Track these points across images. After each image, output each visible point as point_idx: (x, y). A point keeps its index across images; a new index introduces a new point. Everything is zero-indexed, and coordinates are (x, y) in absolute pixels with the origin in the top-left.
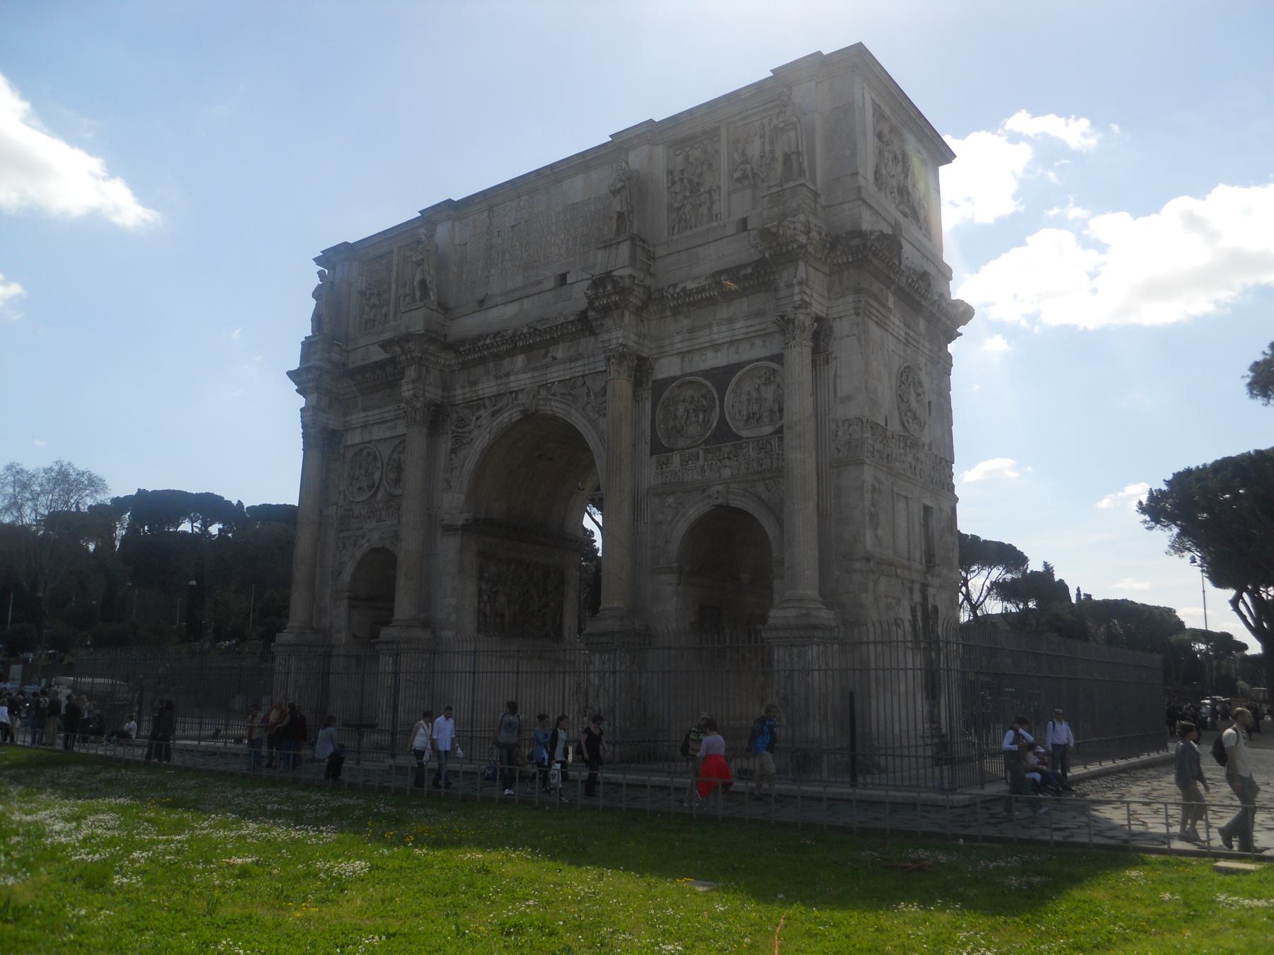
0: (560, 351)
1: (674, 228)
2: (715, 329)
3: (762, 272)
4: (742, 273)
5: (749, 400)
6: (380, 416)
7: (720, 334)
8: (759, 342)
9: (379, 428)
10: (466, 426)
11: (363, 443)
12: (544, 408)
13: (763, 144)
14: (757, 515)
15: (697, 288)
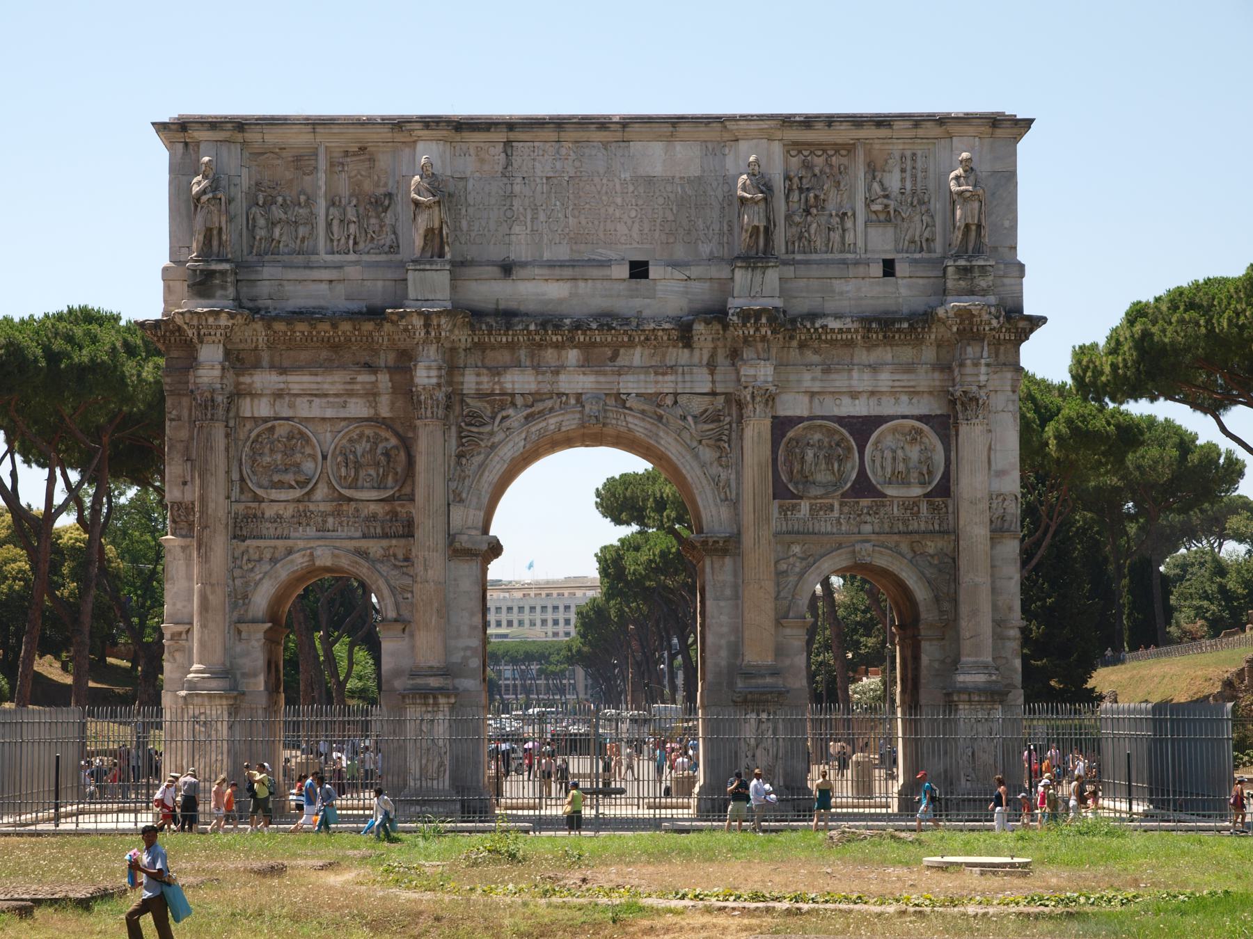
0: (637, 356)
1: (793, 243)
2: (855, 374)
3: (919, 330)
4: (897, 326)
5: (894, 459)
6: (315, 386)
7: (861, 380)
8: (904, 398)
9: (310, 402)
10: (485, 424)
11: (276, 419)
12: (614, 422)
13: (903, 180)
14: (903, 576)
15: (841, 329)
